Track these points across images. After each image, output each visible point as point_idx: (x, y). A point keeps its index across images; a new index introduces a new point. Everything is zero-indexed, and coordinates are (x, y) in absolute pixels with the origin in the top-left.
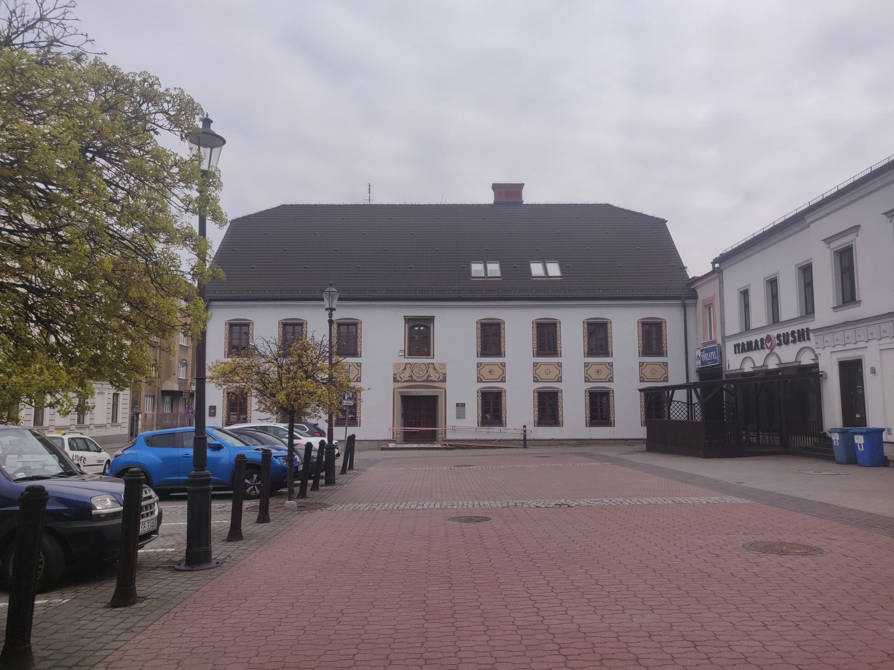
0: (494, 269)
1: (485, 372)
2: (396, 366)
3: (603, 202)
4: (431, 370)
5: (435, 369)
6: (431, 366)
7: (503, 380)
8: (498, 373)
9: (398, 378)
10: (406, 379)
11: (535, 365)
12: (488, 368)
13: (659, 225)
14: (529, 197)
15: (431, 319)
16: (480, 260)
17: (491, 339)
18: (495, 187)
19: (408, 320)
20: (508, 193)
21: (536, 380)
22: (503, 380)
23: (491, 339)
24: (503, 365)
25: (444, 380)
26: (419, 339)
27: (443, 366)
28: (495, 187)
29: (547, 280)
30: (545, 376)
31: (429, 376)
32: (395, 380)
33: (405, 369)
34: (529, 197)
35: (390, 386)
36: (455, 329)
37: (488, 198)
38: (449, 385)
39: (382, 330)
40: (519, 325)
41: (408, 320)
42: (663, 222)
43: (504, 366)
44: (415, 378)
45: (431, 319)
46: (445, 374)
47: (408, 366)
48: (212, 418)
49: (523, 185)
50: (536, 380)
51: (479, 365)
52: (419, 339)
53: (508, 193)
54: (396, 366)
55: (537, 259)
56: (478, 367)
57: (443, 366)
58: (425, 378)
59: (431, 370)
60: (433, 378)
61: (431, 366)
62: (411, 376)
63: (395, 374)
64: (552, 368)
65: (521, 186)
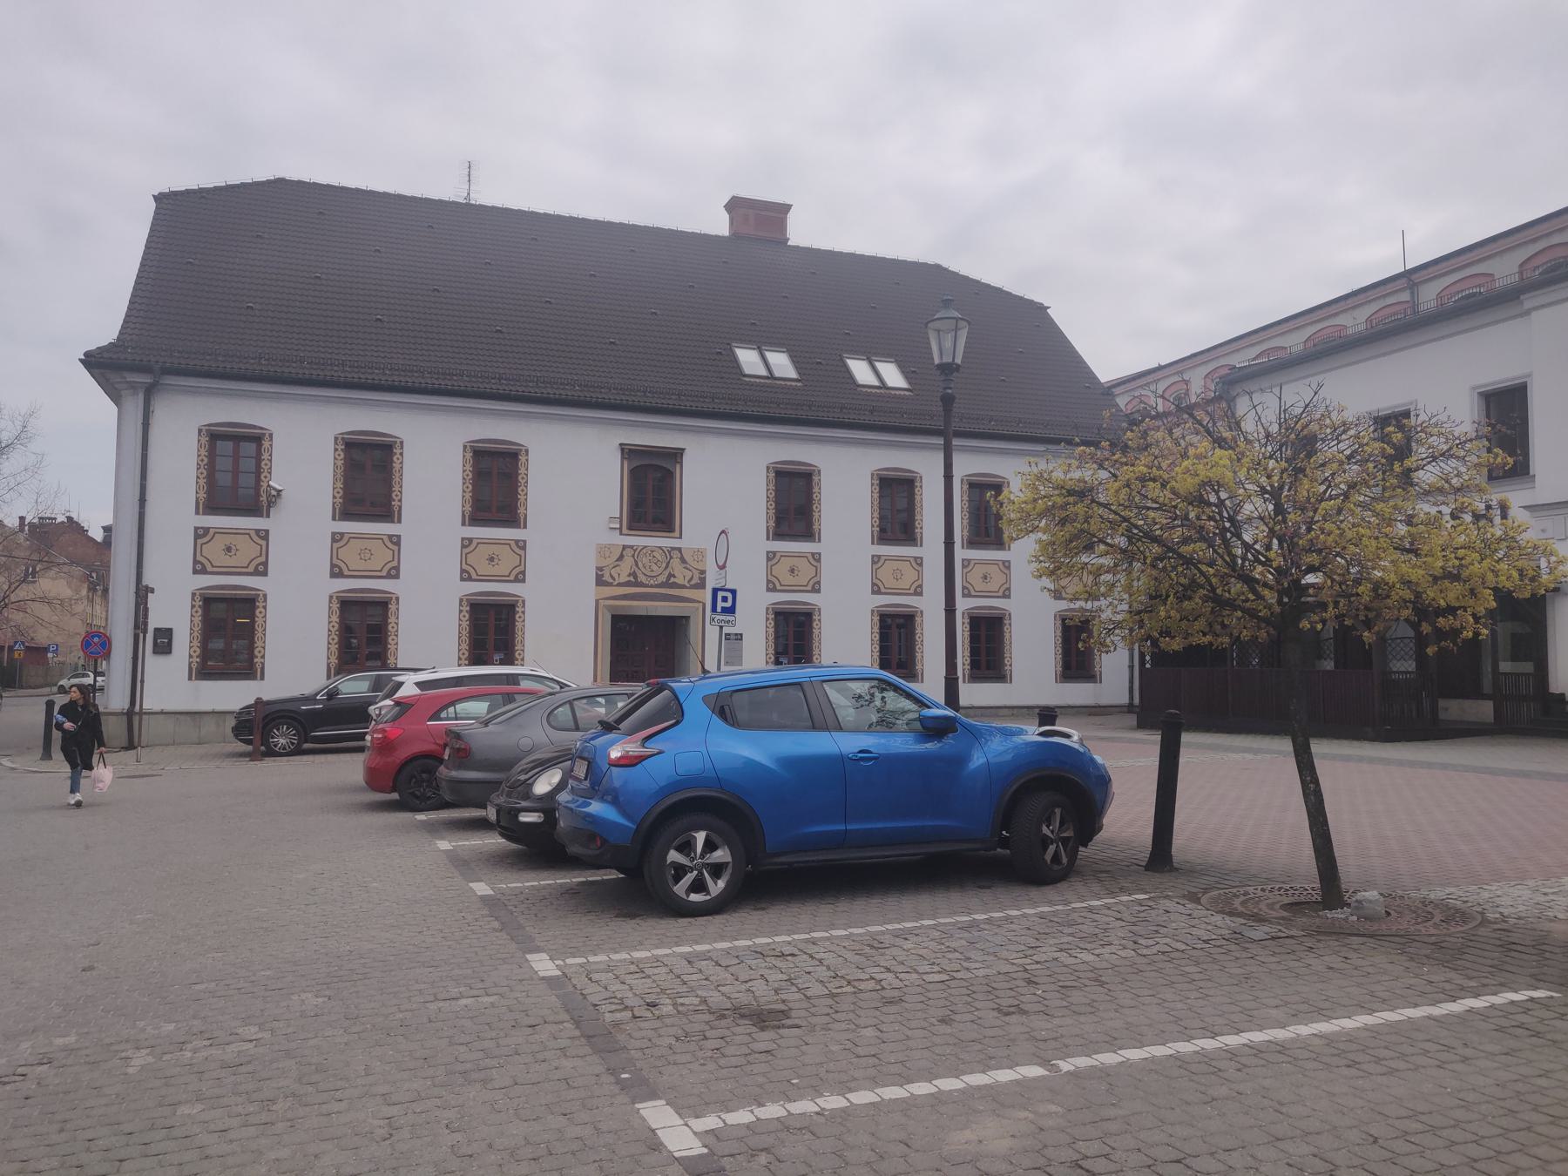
2: (602, 550)
3: (931, 260)
4: (676, 563)
5: (683, 561)
6: (676, 554)
7: (816, 589)
9: (607, 578)
10: (624, 578)
11: (876, 559)
13: (1042, 309)
16: (750, 342)
17: (794, 503)
18: (736, 206)
20: (759, 219)
21: (876, 590)
22: (816, 589)
23: (794, 503)
26: (652, 494)
28: (736, 206)
30: (893, 584)
31: (671, 575)
32: (600, 582)
33: (621, 557)
34: (802, 232)
35: (589, 593)
36: (724, 479)
37: (718, 224)
39: (574, 468)
40: (846, 477)
41: (628, 452)
43: (819, 561)
44: (642, 578)
45: (676, 455)
46: (703, 572)
47: (629, 552)
48: (162, 659)
49: (788, 207)
50: (876, 590)
51: (771, 556)
52: (652, 494)
53: (759, 219)
54: (602, 550)
56: (769, 559)
58: (662, 579)
59: (676, 563)
60: (680, 580)
61: (676, 554)
62: (634, 574)
63: (599, 569)
64: (905, 567)
65: (786, 208)
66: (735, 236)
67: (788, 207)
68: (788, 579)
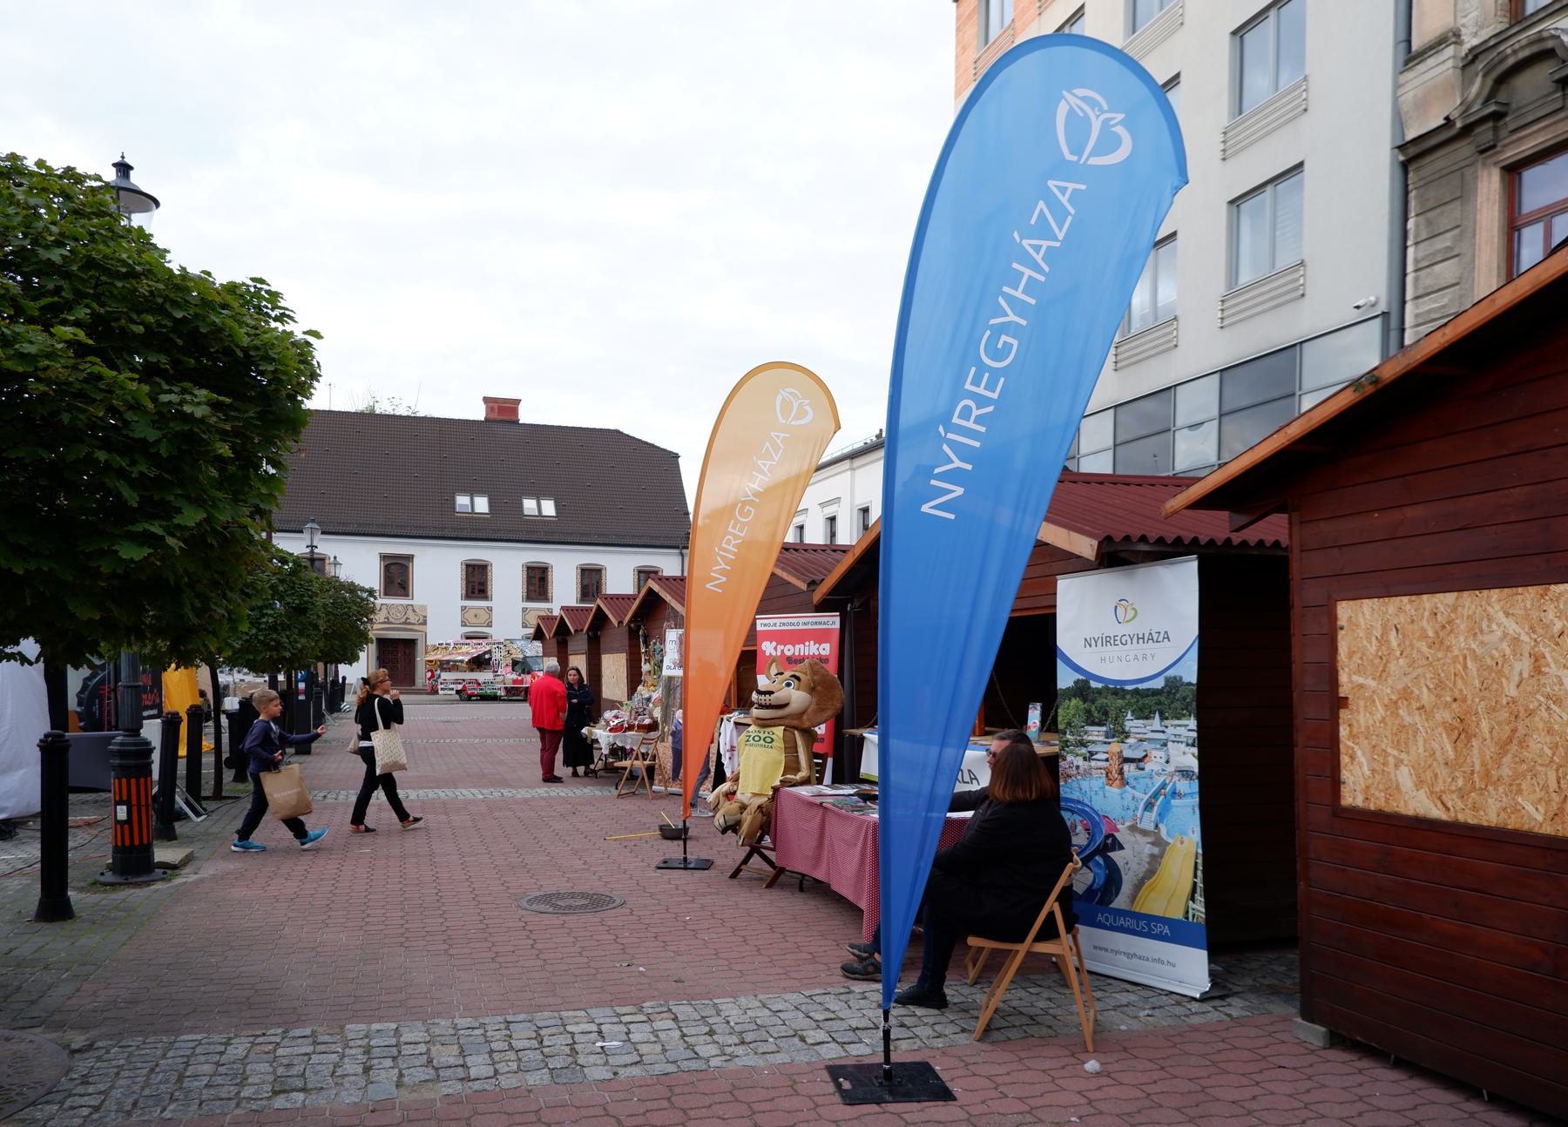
0: (482, 505)
1: (470, 616)
4: (410, 612)
8: (483, 617)
12: (472, 612)
14: (526, 416)
15: (410, 558)
17: (477, 582)
18: (486, 400)
19: (384, 557)
20: (503, 411)
22: (489, 625)
23: (477, 582)
24: (490, 609)
25: (425, 623)
27: (424, 608)
29: (541, 521)
34: (526, 416)
37: (478, 413)
38: (429, 628)
40: (507, 566)
41: (384, 557)
42: (676, 456)
45: (410, 558)
49: (518, 401)
51: (463, 609)
53: (503, 411)
55: (530, 495)
57: (424, 608)
59: (410, 612)
66: (487, 420)
67: (518, 401)
68: (473, 620)
